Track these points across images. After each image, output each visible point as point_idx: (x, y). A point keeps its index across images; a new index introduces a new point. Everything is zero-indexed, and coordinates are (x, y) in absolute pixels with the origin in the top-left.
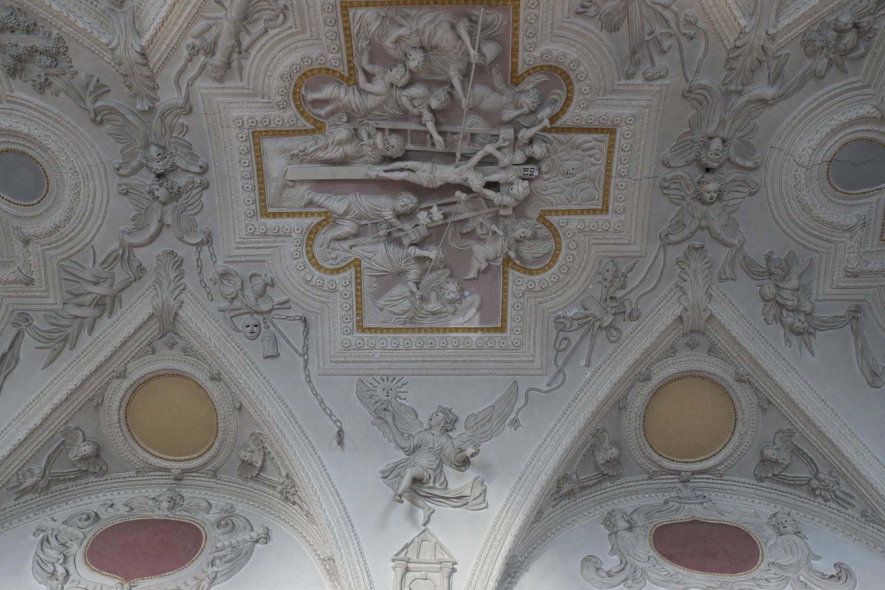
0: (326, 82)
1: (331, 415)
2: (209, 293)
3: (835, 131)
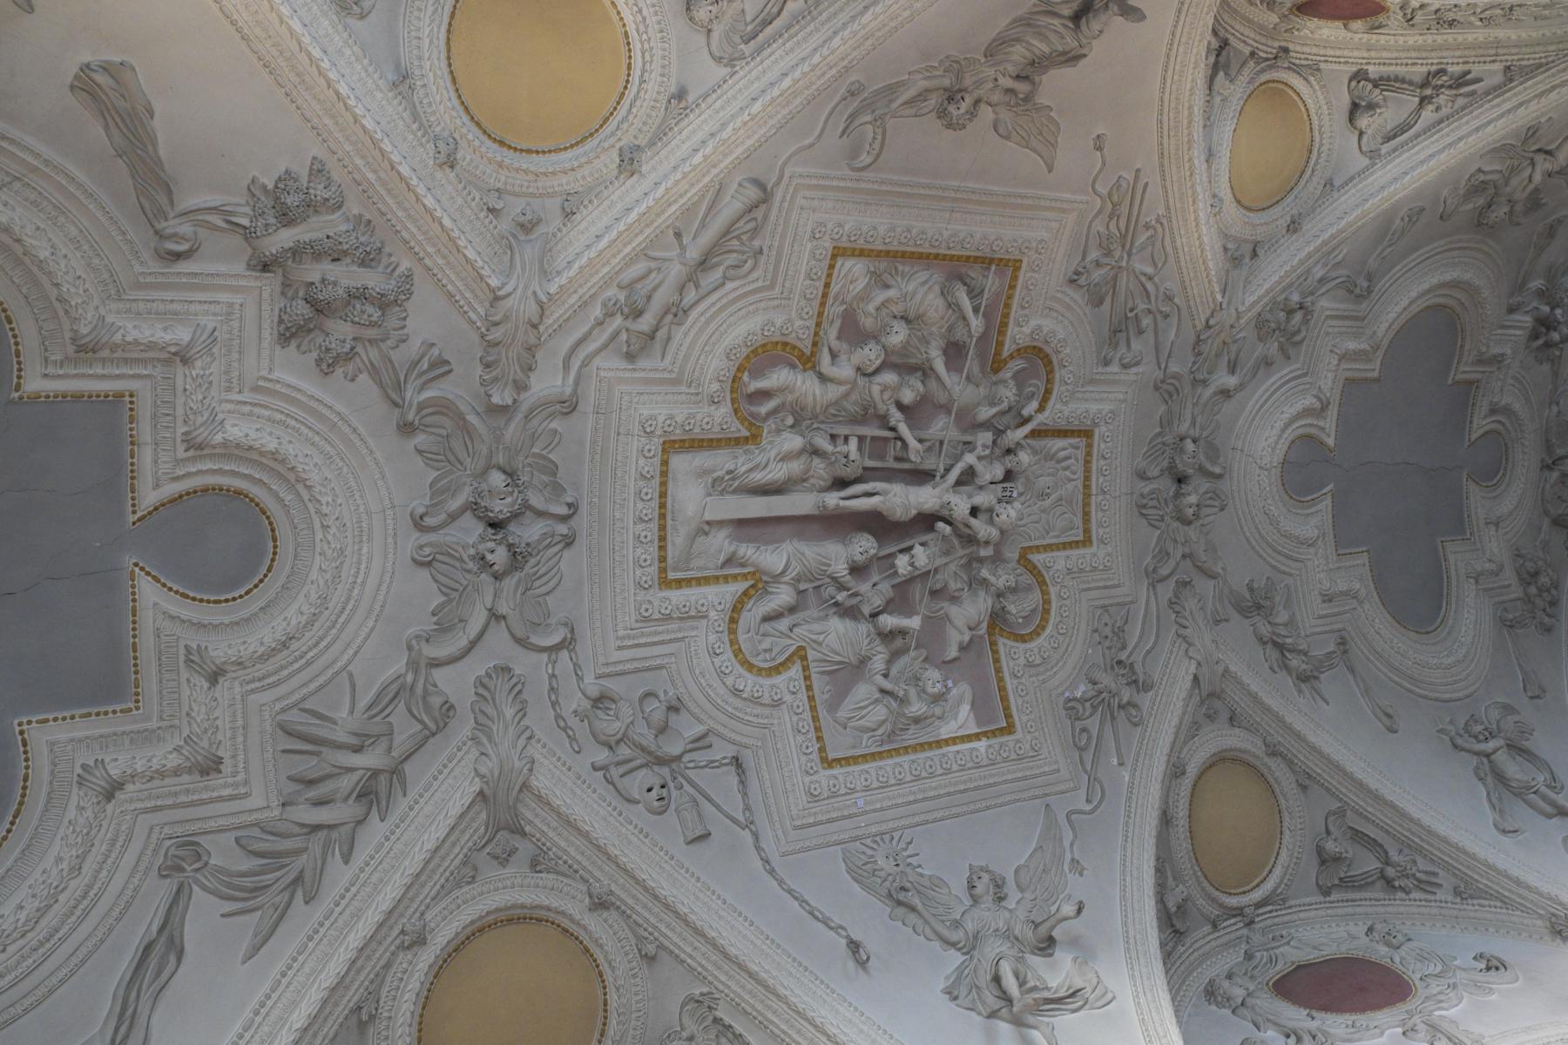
0: (774, 362)
2: (572, 739)
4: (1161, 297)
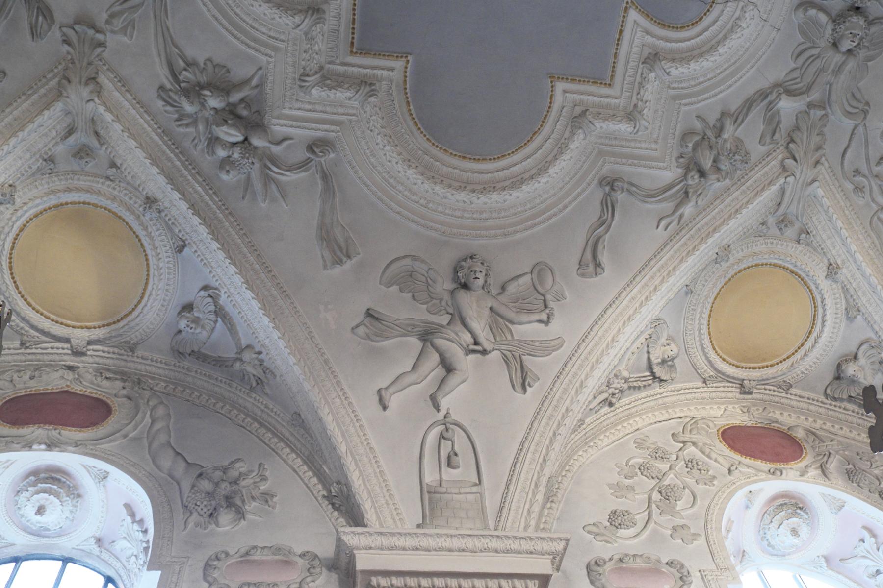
3: (711, 48)
4: (867, 189)
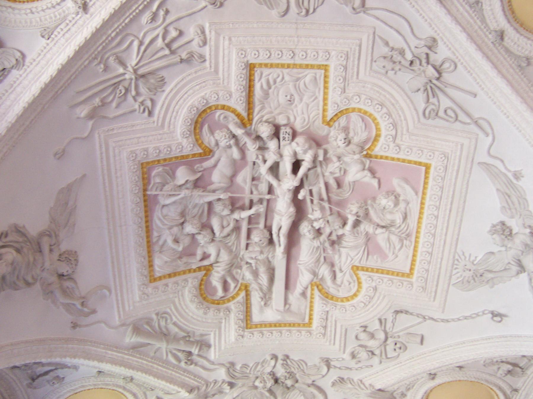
1: (477, 315)
2: (367, 367)
4: (154, 25)
